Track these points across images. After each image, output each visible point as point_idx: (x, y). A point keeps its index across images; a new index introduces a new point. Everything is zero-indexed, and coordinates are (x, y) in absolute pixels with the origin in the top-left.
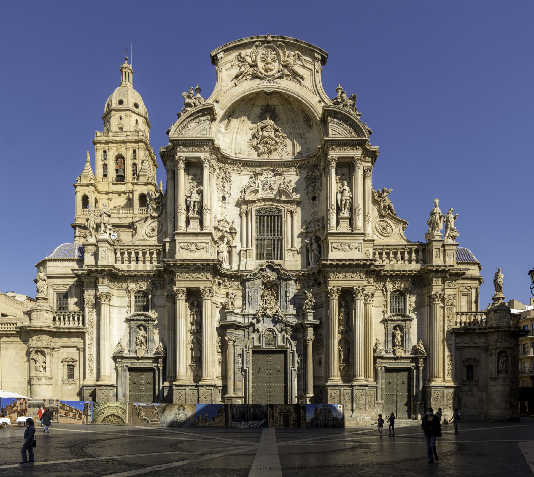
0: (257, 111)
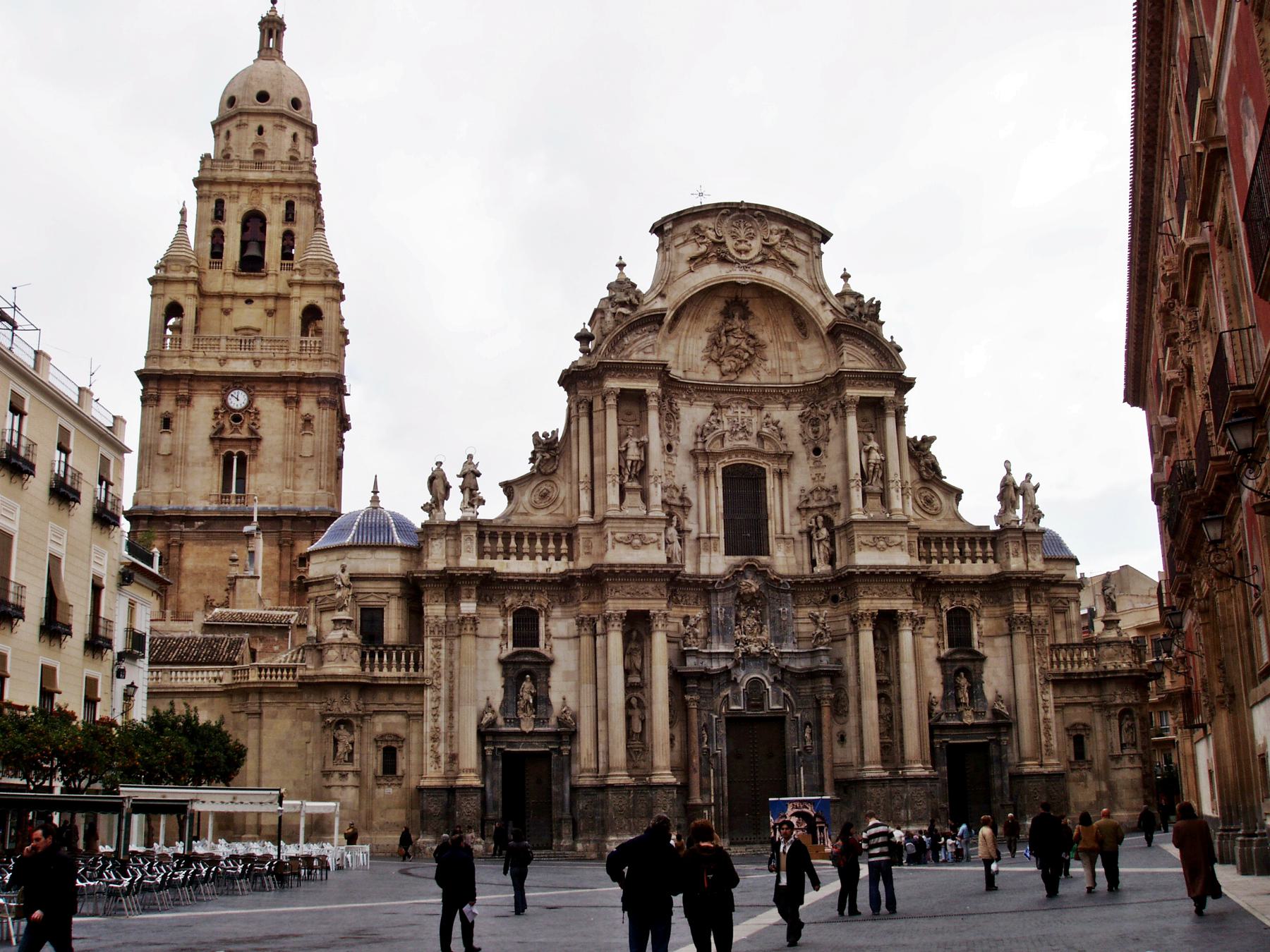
0: (719, 305)
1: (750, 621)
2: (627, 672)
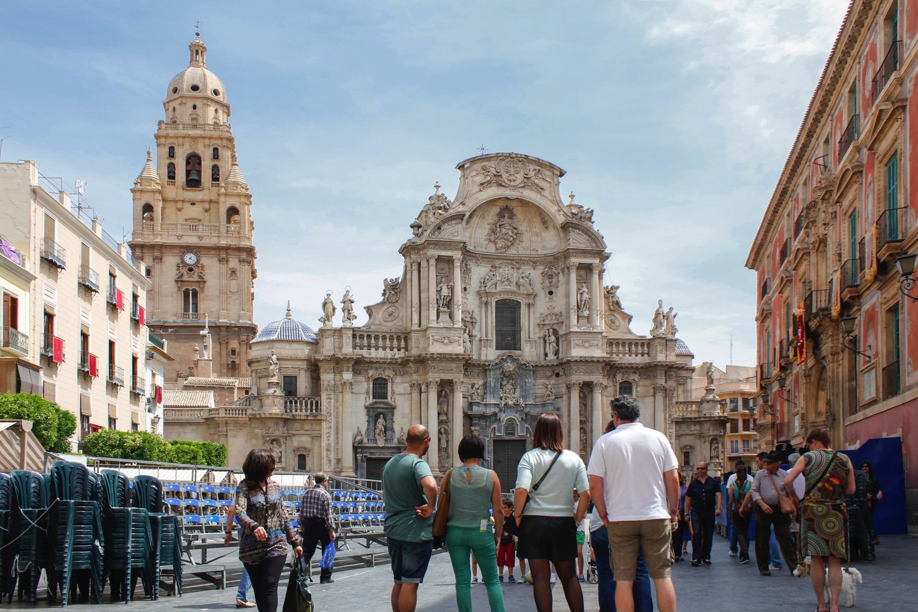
1: (509, 387)
2: (439, 414)
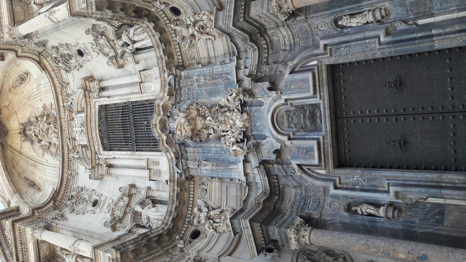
0: (27, 147)
